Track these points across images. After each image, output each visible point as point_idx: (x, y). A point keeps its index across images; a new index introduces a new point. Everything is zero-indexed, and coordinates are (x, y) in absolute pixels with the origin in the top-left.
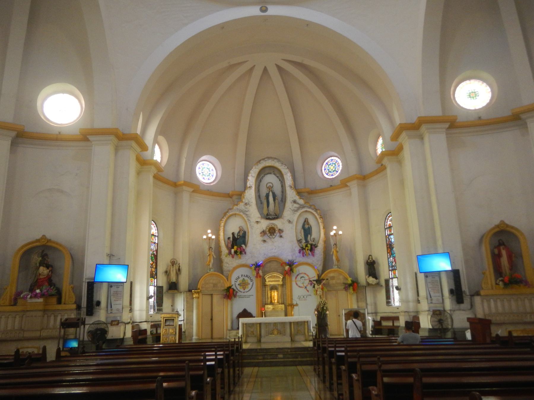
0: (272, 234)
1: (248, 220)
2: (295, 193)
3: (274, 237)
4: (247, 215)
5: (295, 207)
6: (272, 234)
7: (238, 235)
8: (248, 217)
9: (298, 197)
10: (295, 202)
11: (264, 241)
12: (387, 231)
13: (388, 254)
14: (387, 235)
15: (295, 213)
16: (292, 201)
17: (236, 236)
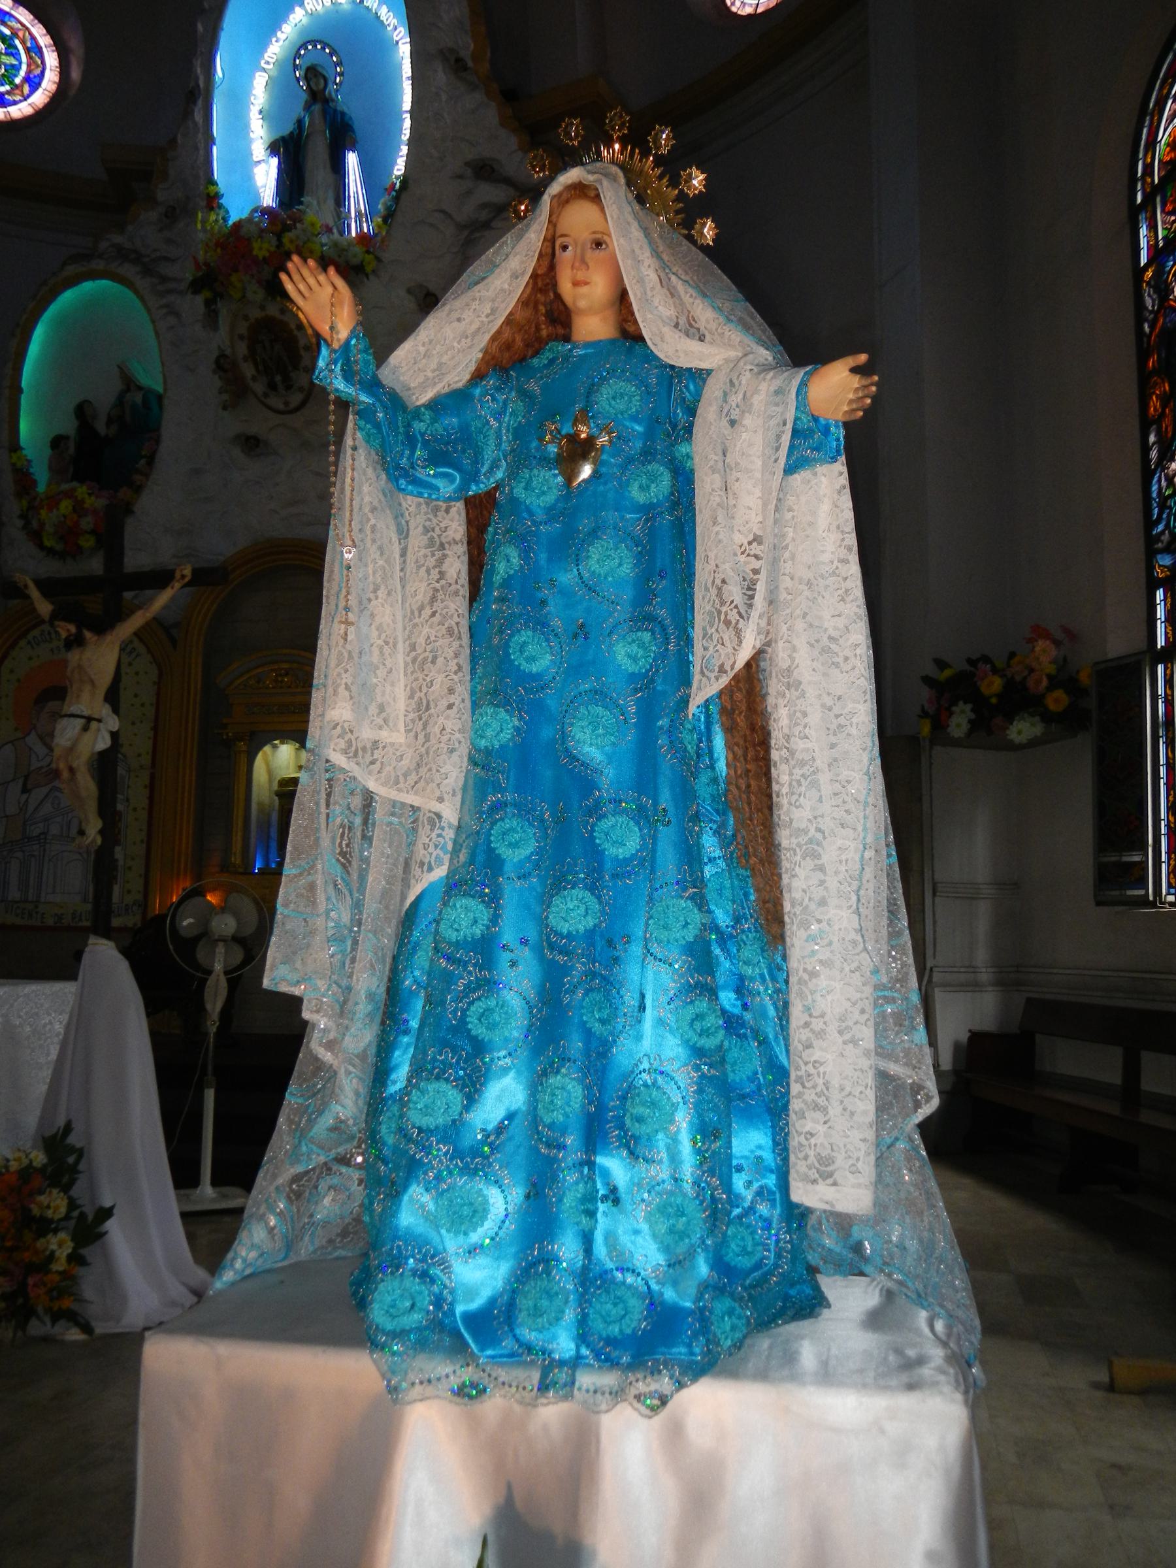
0: (278, 378)
1: (164, 311)
2: (491, 114)
3: (296, 399)
4: (164, 279)
5: (484, 206)
6: (278, 378)
7: (110, 421)
8: (170, 291)
9: (513, 141)
10: (484, 170)
11: (252, 444)
12: (1153, 227)
13: (1152, 439)
14: (1144, 260)
15: (478, 235)
16: (467, 164)
17: (101, 428)
